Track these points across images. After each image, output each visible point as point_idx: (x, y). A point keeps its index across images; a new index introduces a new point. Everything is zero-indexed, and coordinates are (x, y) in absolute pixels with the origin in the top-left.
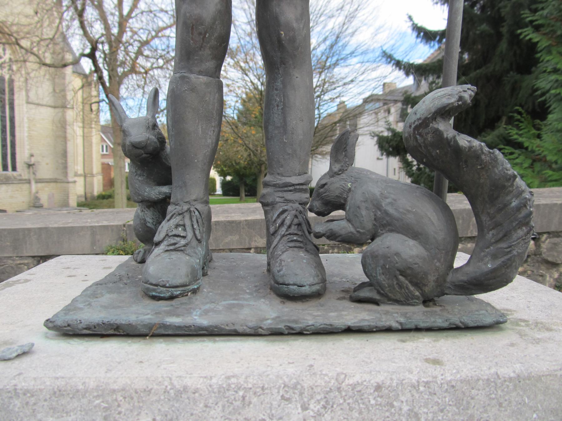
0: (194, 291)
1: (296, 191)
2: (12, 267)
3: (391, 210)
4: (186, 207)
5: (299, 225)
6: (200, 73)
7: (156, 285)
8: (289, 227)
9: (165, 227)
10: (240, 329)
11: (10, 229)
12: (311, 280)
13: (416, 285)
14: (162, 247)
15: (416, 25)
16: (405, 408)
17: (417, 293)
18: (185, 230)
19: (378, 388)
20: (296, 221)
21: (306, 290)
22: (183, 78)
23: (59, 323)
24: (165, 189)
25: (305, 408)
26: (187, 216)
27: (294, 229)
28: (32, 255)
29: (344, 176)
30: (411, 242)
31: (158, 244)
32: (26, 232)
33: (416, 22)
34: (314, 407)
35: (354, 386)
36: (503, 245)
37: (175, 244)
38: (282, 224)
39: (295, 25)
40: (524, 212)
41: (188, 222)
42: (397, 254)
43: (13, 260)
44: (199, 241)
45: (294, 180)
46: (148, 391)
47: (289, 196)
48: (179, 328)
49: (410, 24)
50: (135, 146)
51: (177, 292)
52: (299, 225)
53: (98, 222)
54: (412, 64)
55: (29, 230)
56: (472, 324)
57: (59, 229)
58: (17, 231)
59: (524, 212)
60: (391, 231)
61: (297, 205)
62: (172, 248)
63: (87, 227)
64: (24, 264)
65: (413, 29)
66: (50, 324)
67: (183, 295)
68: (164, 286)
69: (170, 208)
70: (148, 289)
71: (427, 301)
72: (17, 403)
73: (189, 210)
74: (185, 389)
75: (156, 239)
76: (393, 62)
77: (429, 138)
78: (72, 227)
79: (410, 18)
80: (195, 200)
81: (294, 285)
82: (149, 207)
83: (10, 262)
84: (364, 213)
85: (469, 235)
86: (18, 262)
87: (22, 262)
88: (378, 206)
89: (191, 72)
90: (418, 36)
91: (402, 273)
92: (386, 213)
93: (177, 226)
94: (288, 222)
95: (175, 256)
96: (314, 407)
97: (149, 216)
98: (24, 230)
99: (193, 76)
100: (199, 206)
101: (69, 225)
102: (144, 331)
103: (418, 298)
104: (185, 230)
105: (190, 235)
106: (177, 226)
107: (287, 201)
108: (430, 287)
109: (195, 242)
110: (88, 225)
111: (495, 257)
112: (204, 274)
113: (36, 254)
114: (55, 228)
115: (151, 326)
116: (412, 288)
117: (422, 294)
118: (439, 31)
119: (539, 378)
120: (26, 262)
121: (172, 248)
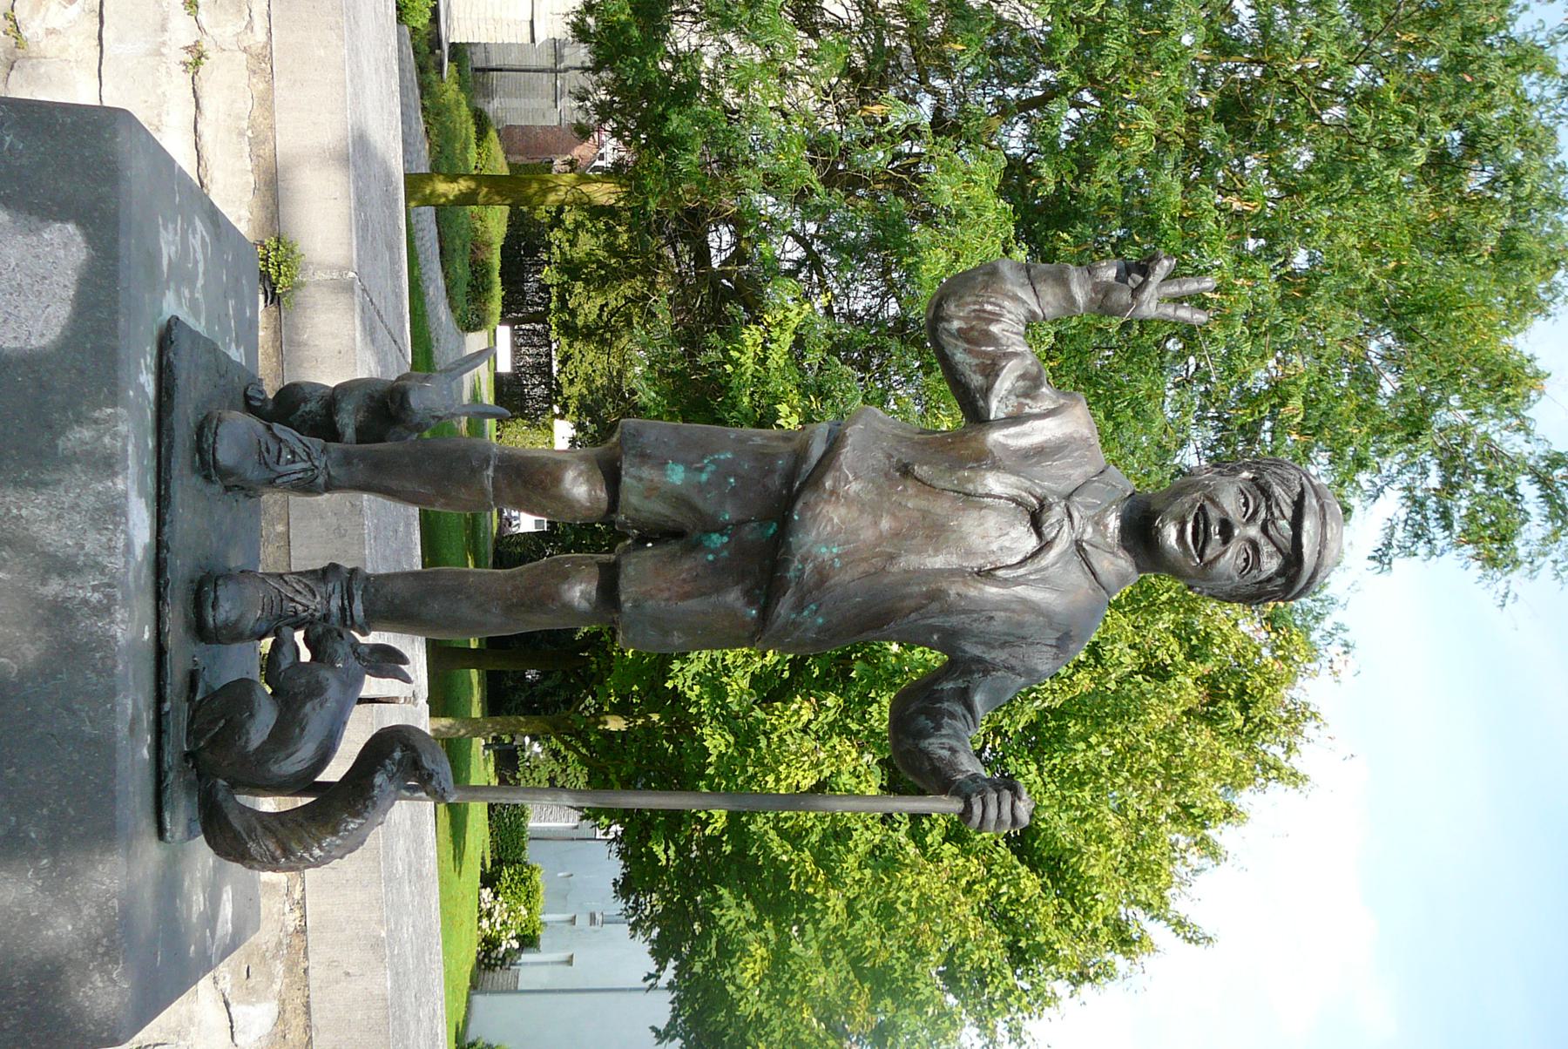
0: (208, 478)
7: (216, 433)
8: (292, 600)
13: (213, 741)
17: (202, 744)
18: (288, 462)
20: (300, 608)
29: (352, 660)
36: (259, 830)
37: (268, 450)
42: (252, 716)
62: (263, 449)
68: (215, 442)
70: (211, 421)
80: (329, 474)
81: (216, 598)
89: (496, 469)
93: (293, 453)
99: (490, 472)
100: (321, 480)
103: (196, 745)
104: (288, 462)
112: (227, 489)
117: (203, 749)
121: (263, 449)
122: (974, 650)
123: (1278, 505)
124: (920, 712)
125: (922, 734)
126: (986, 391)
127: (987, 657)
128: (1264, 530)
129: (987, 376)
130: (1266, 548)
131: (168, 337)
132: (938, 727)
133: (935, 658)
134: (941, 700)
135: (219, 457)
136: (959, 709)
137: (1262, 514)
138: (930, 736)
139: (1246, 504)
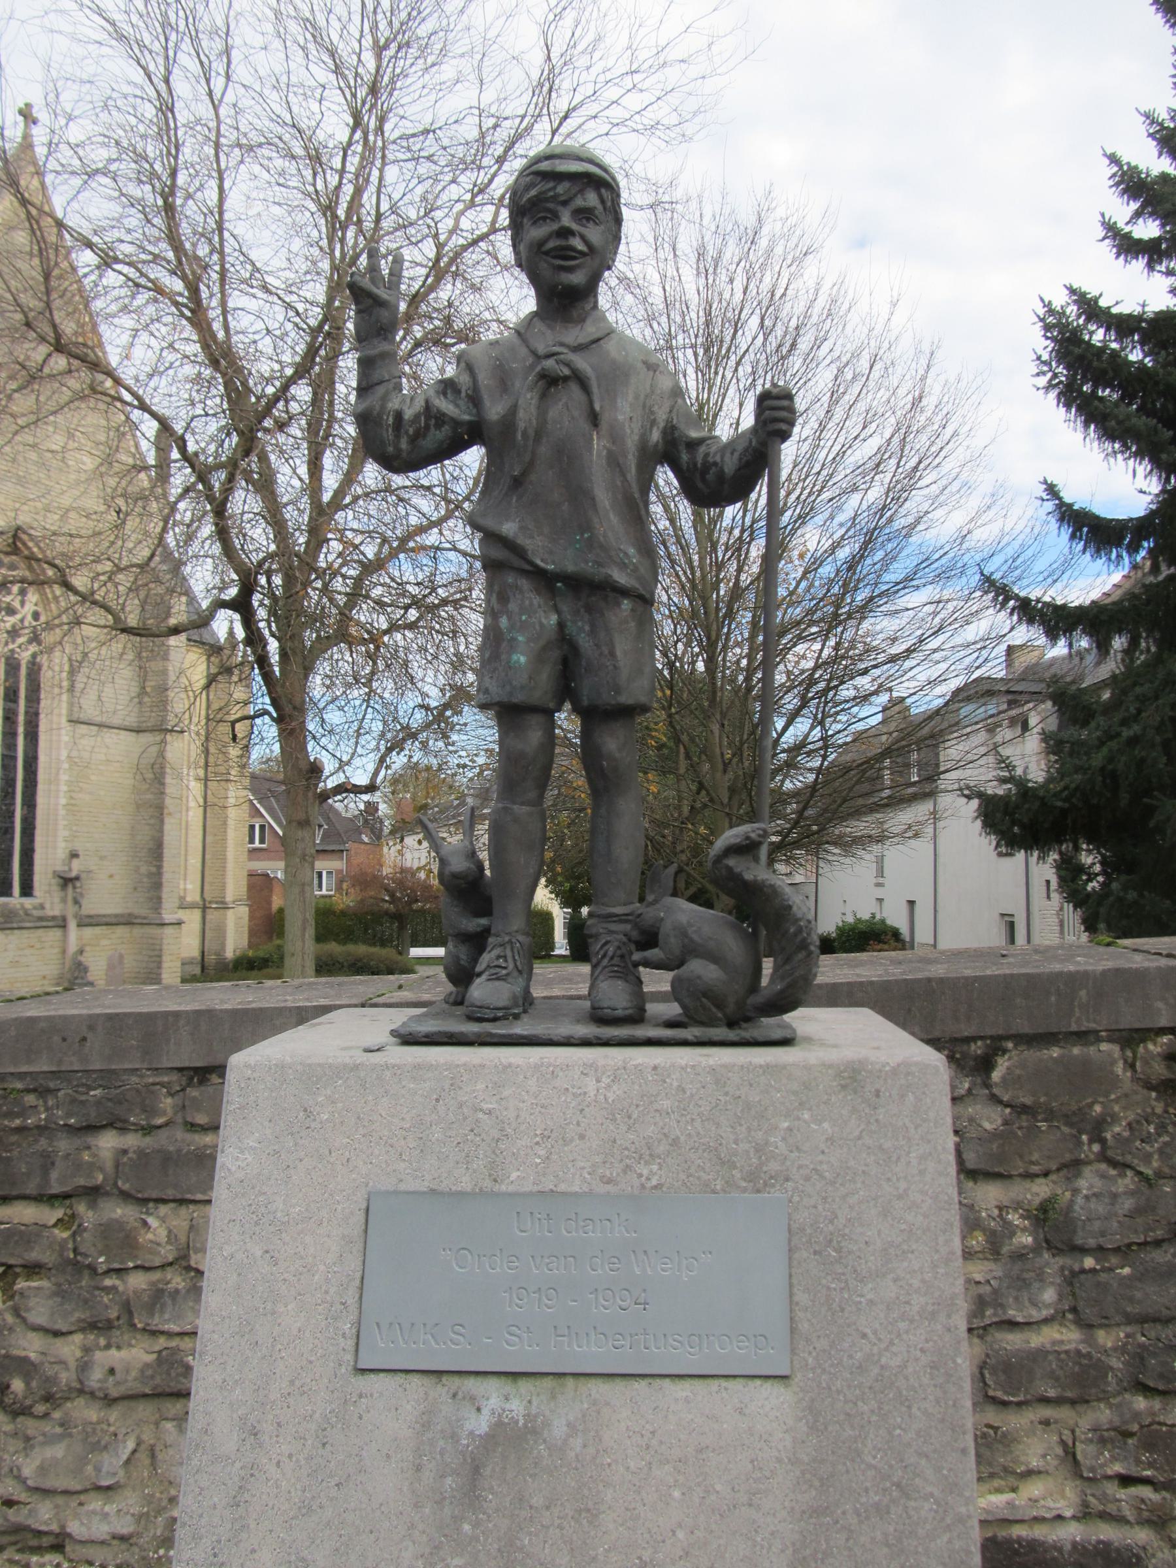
1: (621, 921)
2: (138, 1091)
3: (695, 937)
4: (507, 939)
5: (622, 956)
6: (522, 804)
9: (486, 959)
10: (555, 1039)
11: (140, 1014)
12: (625, 1004)
13: (718, 1007)
14: (484, 977)
15: (1070, 506)
16: (675, 1084)
17: (720, 1015)
19: (655, 1068)
21: (620, 1013)
22: (505, 809)
23: (402, 1031)
24: (484, 921)
25: (598, 1081)
26: (508, 947)
27: (616, 960)
28: (179, 1065)
30: (713, 967)
31: (479, 975)
32: (171, 1019)
33: (1068, 499)
34: (605, 1080)
35: (636, 1066)
36: (787, 967)
38: (604, 956)
39: (617, 755)
40: (799, 938)
41: (509, 953)
42: (699, 977)
43: (142, 1076)
44: (520, 972)
45: (618, 910)
46: (483, 1066)
47: (613, 927)
48: (503, 1036)
49: (1050, 506)
50: (455, 876)
51: (500, 1014)
52: (622, 956)
53: (307, 1000)
54: (1064, 607)
55: (177, 1015)
56: (761, 1039)
57: (234, 1013)
58: (151, 1017)
59: (799, 938)
60: (696, 956)
61: (621, 937)
63: (290, 1009)
64: (162, 1085)
65: (1061, 520)
66: (394, 1033)
67: (505, 1018)
69: (491, 940)
71: (731, 1024)
72: (388, 1073)
73: (510, 942)
74: (510, 1065)
75: (478, 969)
76: (1012, 603)
77: (724, 872)
78: (261, 1009)
79: (1052, 490)
82: (463, 942)
83: (134, 1079)
84: (672, 940)
85: (1074, 1028)
86: (151, 1080)
87: (157, 1080)
88: (684, 934)
89: (514, 803)
90: (1073, 537)
91: (705, 995)
92: (692, 940)
93: (498, 957)
94: (610, 953)
95: (497, 983)
96: (605, 1080)
97: (463, 952)
98: (166, 1014)
101: (254, 1005)
102: (473, 1038)
105: (511, 966)
106: (498, 957)
107: (611, 932)
108: (731, 1008)
109: (516, 974)
110: (289, 1004)
111: (782, 978)
113: (187, 1064)
114: (226, 1011)
115: (478, 1035)
116: (714, 1010)
117: (725, 1015)
118: (1131, 519)
119: (784, 1067)
120: (166, 1079)
122: (656, 436)
123: (544, 192)
124: (704, 480)
125: (721, 475)
126: (456, 423)
127: (662, 425)
128: (565, 203)
129: (444, 423)
130: (579, 202)
131: (408, 1039)
132: (715, 464)
133: (665, 477)
134: (695, 464)
135: (501, 1004)
136: (702, 449)
137: (551, 205)
138: (722, 471)
139: (544, 219)
